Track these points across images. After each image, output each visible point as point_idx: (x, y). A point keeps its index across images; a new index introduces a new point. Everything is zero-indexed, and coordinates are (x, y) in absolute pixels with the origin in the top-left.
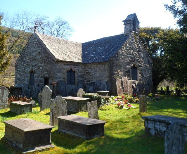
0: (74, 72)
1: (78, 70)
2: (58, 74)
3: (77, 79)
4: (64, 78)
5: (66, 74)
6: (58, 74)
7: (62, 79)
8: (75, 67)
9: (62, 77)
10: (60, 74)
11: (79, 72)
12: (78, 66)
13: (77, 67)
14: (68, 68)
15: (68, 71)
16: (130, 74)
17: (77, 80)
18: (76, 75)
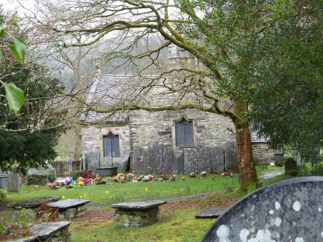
0: (117, 136)
1: (124, 133)
2: (86, 142)
3: (123, 148)
4: (98, 148)
5: (101, 142)
6: (86, 142)
7: (94, 149)
8: (116, 129)
9: (95, 146)
10: (90, 143)
11: (127, 136)
12: (123, 127)
13: (120, 128)
14: (105, 131)
15: (104, 137)
16: (171, 137)
17: (123, 149)
18: (120, 140)
